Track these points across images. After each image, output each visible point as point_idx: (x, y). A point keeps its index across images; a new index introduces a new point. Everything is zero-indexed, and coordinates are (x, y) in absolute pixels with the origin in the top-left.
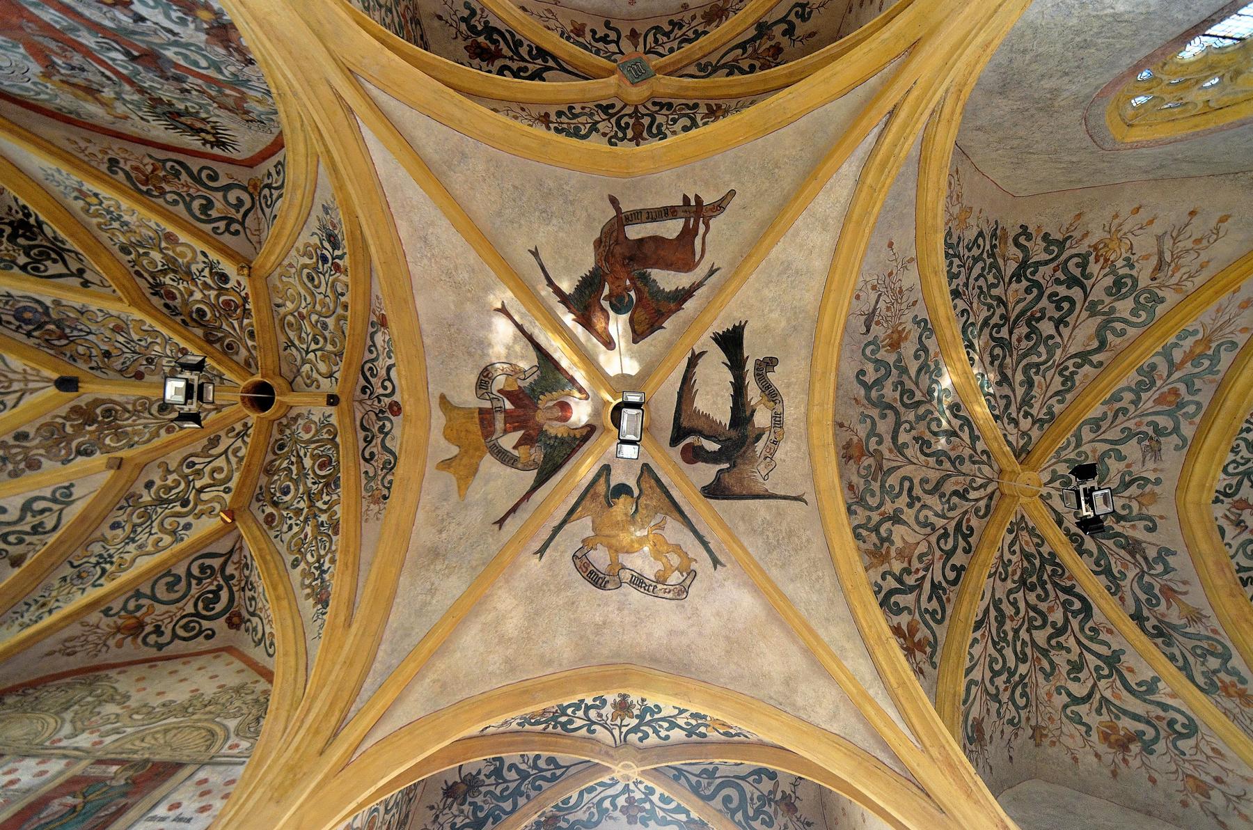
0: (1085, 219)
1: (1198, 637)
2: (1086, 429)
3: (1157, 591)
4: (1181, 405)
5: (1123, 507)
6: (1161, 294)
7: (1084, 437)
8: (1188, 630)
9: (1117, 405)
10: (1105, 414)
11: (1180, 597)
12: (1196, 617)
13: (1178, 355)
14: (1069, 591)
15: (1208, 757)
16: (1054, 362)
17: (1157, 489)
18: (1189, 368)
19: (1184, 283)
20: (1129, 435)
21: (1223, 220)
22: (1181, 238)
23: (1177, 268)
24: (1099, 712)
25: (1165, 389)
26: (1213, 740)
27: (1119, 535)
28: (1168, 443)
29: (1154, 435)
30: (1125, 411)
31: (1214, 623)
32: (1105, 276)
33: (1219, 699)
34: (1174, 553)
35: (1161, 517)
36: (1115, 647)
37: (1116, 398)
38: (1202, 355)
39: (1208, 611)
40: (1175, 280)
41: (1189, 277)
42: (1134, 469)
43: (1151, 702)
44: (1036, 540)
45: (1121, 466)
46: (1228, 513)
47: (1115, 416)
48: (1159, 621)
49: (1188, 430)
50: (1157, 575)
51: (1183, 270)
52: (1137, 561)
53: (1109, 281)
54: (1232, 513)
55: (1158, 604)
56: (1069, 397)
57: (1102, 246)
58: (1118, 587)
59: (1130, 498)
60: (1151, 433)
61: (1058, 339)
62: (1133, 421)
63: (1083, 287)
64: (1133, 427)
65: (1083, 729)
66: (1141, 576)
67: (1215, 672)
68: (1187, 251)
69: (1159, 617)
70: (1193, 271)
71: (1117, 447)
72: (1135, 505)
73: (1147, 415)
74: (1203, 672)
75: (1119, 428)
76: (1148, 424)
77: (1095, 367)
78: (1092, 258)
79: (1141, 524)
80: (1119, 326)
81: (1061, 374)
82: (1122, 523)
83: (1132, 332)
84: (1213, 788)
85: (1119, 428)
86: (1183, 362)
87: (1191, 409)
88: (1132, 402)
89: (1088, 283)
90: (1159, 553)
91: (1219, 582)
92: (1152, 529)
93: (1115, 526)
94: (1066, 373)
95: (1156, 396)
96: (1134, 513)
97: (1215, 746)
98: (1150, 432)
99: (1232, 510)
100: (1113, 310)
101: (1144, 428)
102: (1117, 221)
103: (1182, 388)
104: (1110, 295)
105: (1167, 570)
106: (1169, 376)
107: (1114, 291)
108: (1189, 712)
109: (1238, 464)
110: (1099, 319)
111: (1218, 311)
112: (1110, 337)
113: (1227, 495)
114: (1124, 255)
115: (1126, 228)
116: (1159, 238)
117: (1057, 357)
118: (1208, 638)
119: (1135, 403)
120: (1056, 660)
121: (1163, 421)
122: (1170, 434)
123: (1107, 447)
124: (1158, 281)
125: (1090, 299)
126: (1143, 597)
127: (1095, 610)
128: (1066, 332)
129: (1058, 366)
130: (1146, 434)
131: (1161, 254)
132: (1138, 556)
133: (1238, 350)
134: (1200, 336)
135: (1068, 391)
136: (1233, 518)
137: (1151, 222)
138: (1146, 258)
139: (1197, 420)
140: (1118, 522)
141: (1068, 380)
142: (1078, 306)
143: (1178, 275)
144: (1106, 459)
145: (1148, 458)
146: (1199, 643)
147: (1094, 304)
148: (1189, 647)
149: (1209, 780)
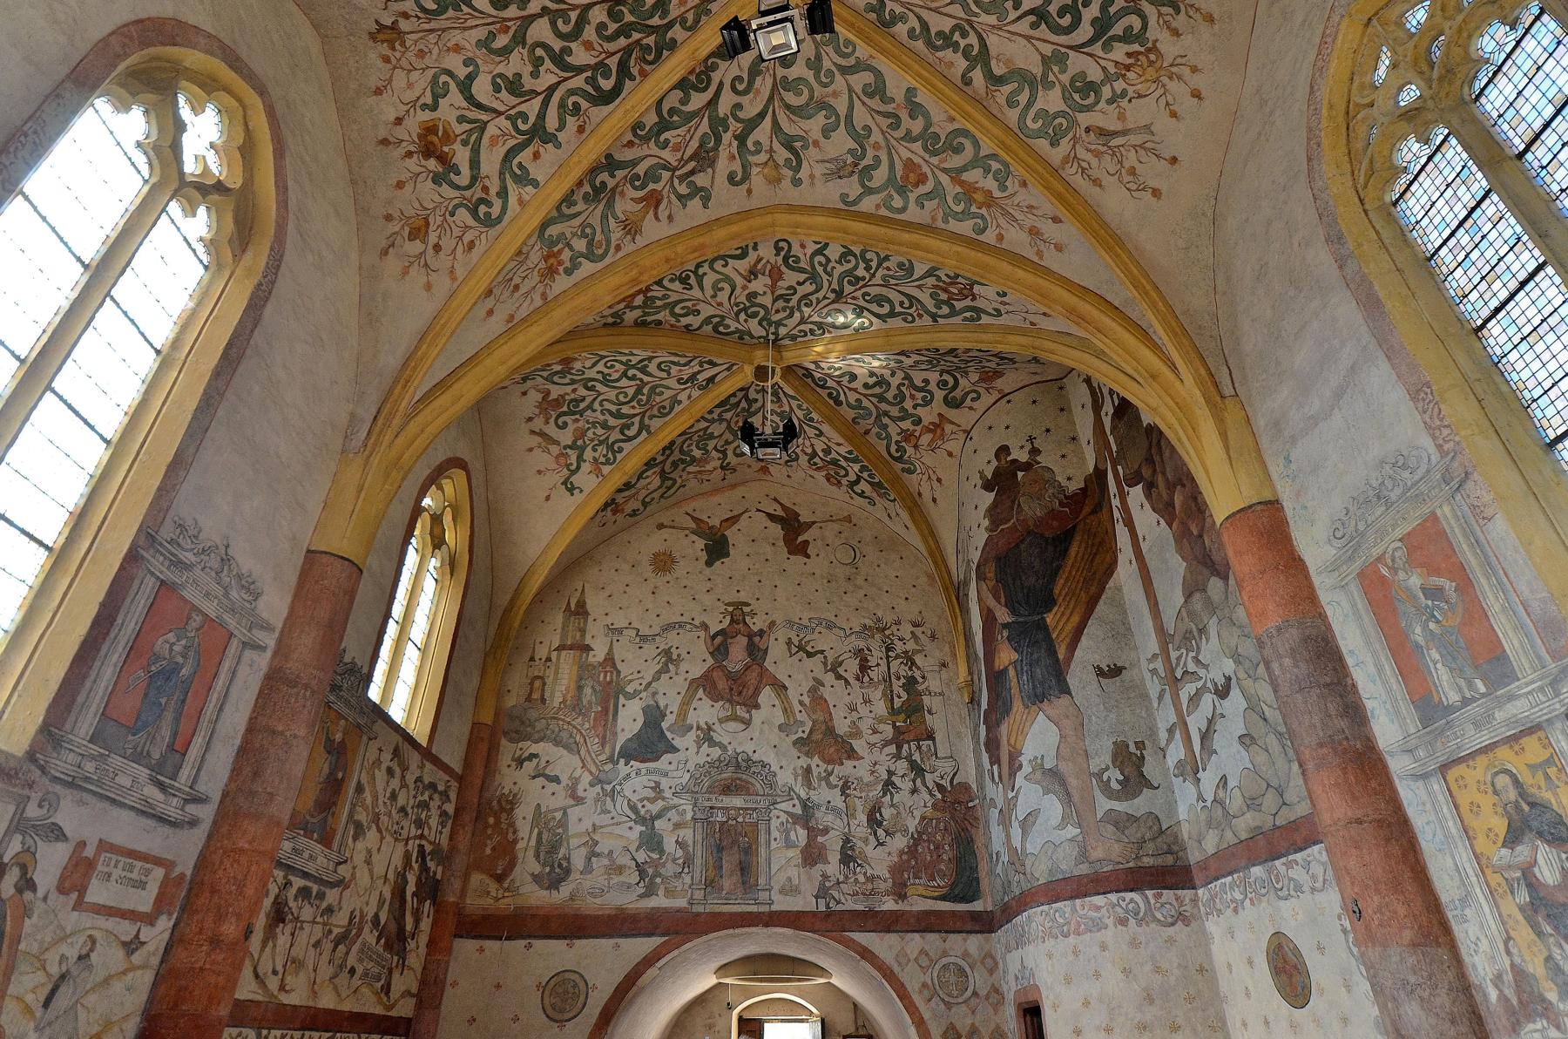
0: (1204, 30)
1: (606, 230)
2: (867, 77)
3: (651, 186)
4: (902, 191)
5: (757, 143)
6: (1064, 142)
7: (856, 76)
8: (611, 220)
9: (904, 115)
10: (892, 100)
11: (651, 213)
12: (631, 228)
13: (972, 176)
14: (624, 71)
15: (460, 238)
16: (976, 15)
17: (786, 183)
18: (952, 190)
19: (1075, 164)
20: (861, 137)
21: (1156, 193)
22: (1141, 152)
23: (1097, 154)
24: (462, 119)
25: (925, 169)
26: (483, 241)
27: (718, 140)
28: (853, 187)
29: (860, 167)
30: (896, 125)
31: (629, 247)
32: (1104, 69)
33: (536, 248)
34: (706, 207)
35: (749, 191)
36: (561, 136)
37: (915, 109)
38: (971, 201)
39: (641, 241)
40: (1081, 153)
41: (1083, 170)
42: (812, 151)
43: (503, 181)
44: (690, 17)
45: (816, 134)
46: (764, 261)
47: (887, 115)
48: (613, 190)
49: (868, 204)
50: (672, 185)
51: (1094, 162)
52: (687, 162)
53: (1095, 74)
54: (765, 266)
55: (635, 188)
56: (920, 45)
57: (1152, 57)
58: (646, 139)
59: (771, 150)
60: (864, 163)
61: (1013, 15)
62: (880, 139)
63: (1091, 42)
64: (872, 139)
65: (428, 99)
66: (666, 166)
67: (569, 245)
68: (1120, 162)
69: (620, 189)
70: (1090, 172)
71: (842, 124)
72: (763, 157)
73: (890, 154)
74: (563, 234)
75: (870, 122)
76: (877, 159)
77: (963, 76)
78: (1136, 47)
79: (737, 166)
80: (1023, 98)
81: (956, 28)
82: (735, 143)
83: (1012, 115)
84: (423, 242)
85: (870, 122)
86: (962, 183)
87: (898, 202)
88: (909, 132)
89: (1097, 49)
90: (702, 189)
91: (680, 249)
92: (731, 178)
93: (729, 134)
94: (956, 36)
95: (917, 160)
96: (750, 158)
97: (477, 243)
98: (868, 161)
99: (769, 267)
100: (1049, 86)
101: (870, 153)
102: (1186, 71)
103: (929, 186)
104: (1073, 80)
105: (680, 197)
106: (944, 170)
107: (1078, 84)
108: (506, 219)
109: (825, 267)
110: (1037, 70)
111: (1031, 207)
112: (1007, 89)
113: (786, 259)
114: (1131, 90)
115: (1173, 86)
116: (1147, 128)
117: (984, 18)
118: (608, 242)
119: (909, 137)
120: (515, 56)
121: (880, 176)
122: (863, 185)
123: (842, 110)
124: (1084, 135)
125: (1071, 53)
126: (641, 169)
127: (606, 109)
128: (1023, 26)
129: (970, 23)
130: (864, 156)
131: (1124, 133)
132: (693, 164)
133: (974, 236)
134: (997, 194)
135: (930, 44)
136: (759, 267)
137: (1174, 115)
138: (1122, 117)
139: (883, 212)
140: (736, 137)
141: (947, 40)
142: (1063, 39)
143: (1089, 156)
144: (824, 112)
145: (828, 165)
146: (598, 230)
147: (1059, 59)
148: (590, 221)
149: (433, 238)
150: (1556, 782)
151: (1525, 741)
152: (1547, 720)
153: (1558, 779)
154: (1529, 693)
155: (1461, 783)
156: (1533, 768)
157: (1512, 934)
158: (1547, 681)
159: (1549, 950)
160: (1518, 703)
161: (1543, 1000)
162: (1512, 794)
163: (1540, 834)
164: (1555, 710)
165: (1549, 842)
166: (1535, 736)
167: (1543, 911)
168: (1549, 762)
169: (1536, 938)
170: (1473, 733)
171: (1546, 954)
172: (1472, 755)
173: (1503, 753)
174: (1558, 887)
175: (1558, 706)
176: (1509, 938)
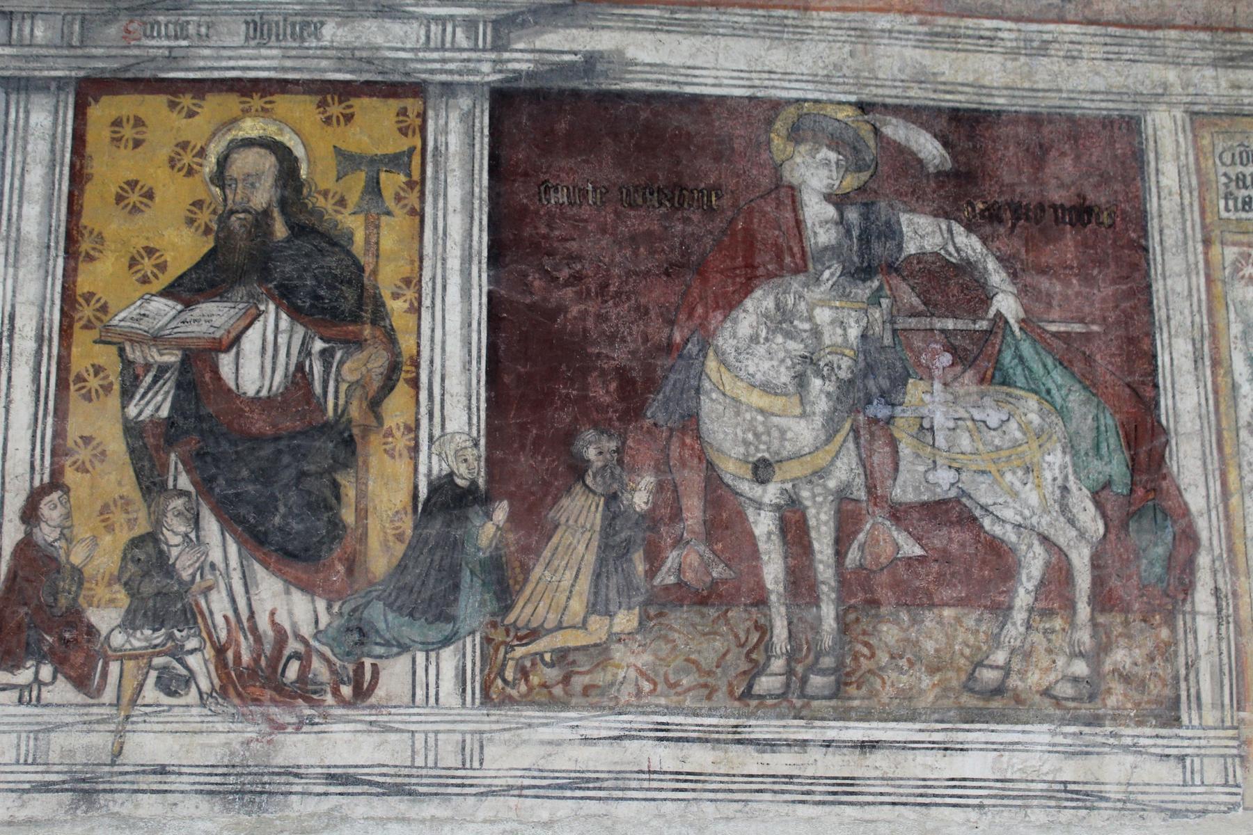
150: (390, 203)
151: (360, 104)
152: (443, 84)
153: (398, 198)
154: (437, 19)
155: (128, 132)
156: (348, 161)
157: (70, 477)
158: (493, 14)
159: (158, 523)
160: (397, 28)
161: (74, 619)
162: (263, 196)
163: (286, 297)
164: (477, 72)
165: (296, 313)
166: (394, 104)
167: (194, 443)
168: (397, 162)
169: (136, 495)
170: (239, 40)
171: (143, 528)
172: (201, 88)
173: (301, 109)
174: (264, 403)
175: (486, 68)
176: (56, 483)
